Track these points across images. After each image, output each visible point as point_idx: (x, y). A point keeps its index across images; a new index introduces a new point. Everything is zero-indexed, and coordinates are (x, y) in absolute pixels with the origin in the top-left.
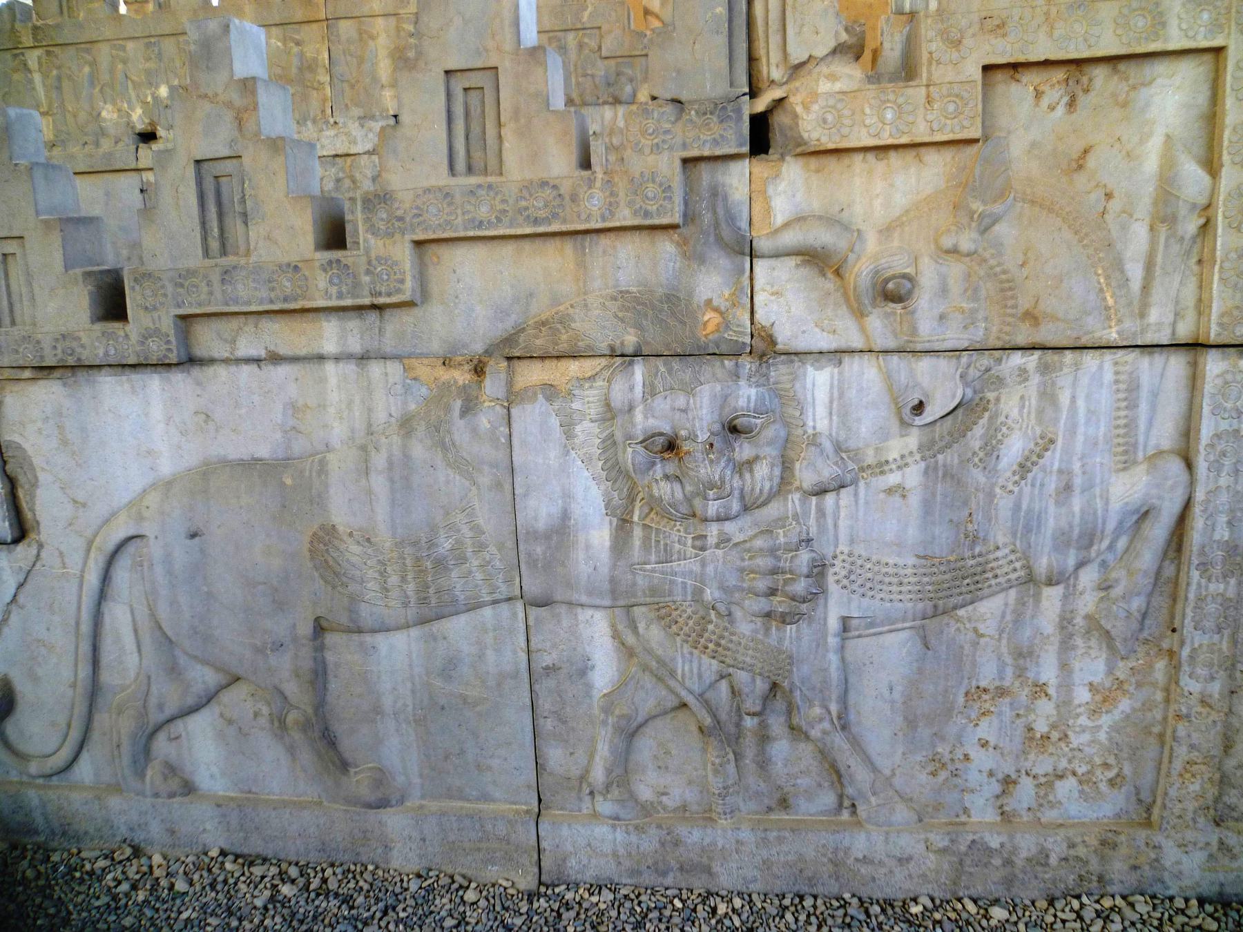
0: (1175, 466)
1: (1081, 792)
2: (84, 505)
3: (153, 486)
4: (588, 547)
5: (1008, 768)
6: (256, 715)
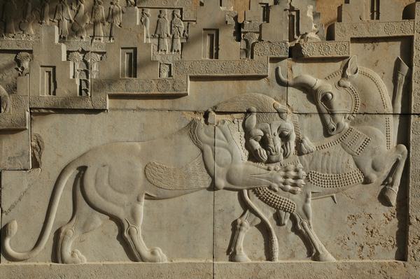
0: (404, 147)
1: (383, 250)
2: (61, 156)
3: (90, 150)
4: (236, 170)
5: (362, 242)
6: (116, 230)
